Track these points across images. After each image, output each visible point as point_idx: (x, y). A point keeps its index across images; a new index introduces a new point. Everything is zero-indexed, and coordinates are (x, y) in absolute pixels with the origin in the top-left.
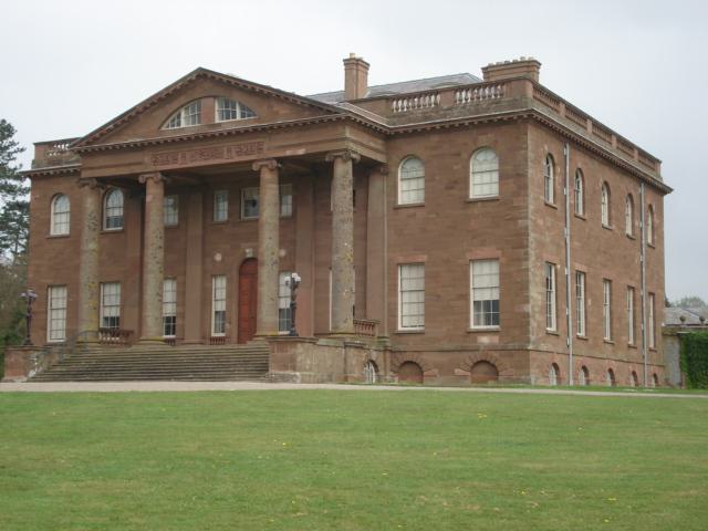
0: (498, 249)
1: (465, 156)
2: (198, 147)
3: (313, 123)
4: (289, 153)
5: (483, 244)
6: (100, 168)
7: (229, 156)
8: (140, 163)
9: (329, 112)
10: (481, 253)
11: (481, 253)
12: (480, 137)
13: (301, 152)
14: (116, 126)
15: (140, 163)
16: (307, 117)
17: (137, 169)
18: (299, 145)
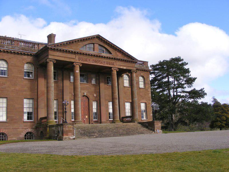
0: (146, 100)
1: (138, 77)
2: (95, 58)
3: (128, 61)
4: (121, 67)
5: (143, 99)
6: (58, 56)
7: (104, 63)
8: (74, 59)
9: (134, 60)
10: (143, 101)
11: (143, 101)
12: (141, 73)
13: (125, 68)
14: (67, 43)
15: (74, 59)
16: (126, 58)
17: (72, 60)
18: (125, 66)
